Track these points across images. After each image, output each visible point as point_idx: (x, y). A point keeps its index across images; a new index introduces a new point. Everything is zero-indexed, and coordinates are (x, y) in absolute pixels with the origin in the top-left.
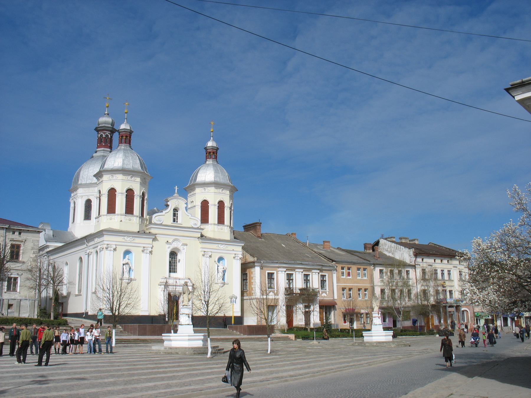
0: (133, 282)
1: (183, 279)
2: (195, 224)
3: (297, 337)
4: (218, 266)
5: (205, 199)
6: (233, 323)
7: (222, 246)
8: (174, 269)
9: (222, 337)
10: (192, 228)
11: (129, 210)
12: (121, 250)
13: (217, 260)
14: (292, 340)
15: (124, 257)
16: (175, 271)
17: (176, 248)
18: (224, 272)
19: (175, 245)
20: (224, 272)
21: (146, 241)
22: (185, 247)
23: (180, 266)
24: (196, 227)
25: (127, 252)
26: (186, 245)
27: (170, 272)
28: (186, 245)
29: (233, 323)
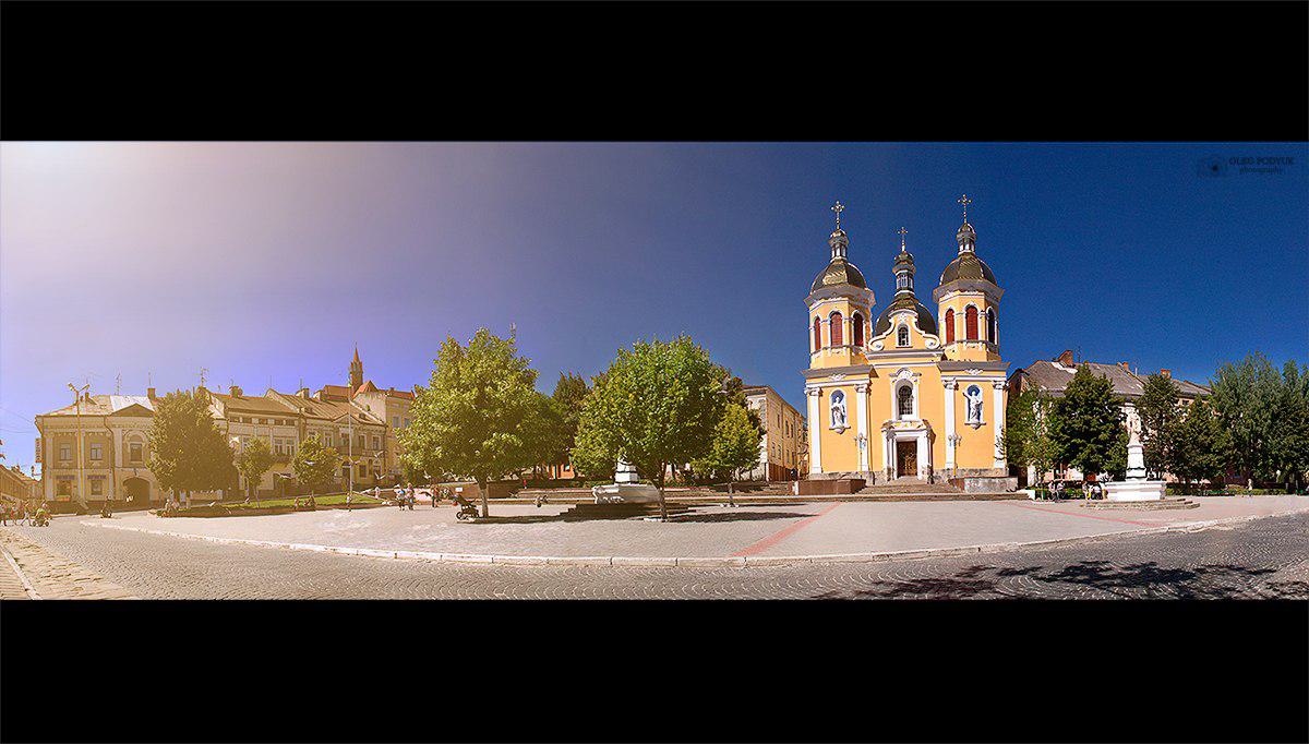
4: (969, 401)
12: (828, 393)
13: (966, 393)
18: (978, 406)
19: (903, 375)
20: (978, 406)
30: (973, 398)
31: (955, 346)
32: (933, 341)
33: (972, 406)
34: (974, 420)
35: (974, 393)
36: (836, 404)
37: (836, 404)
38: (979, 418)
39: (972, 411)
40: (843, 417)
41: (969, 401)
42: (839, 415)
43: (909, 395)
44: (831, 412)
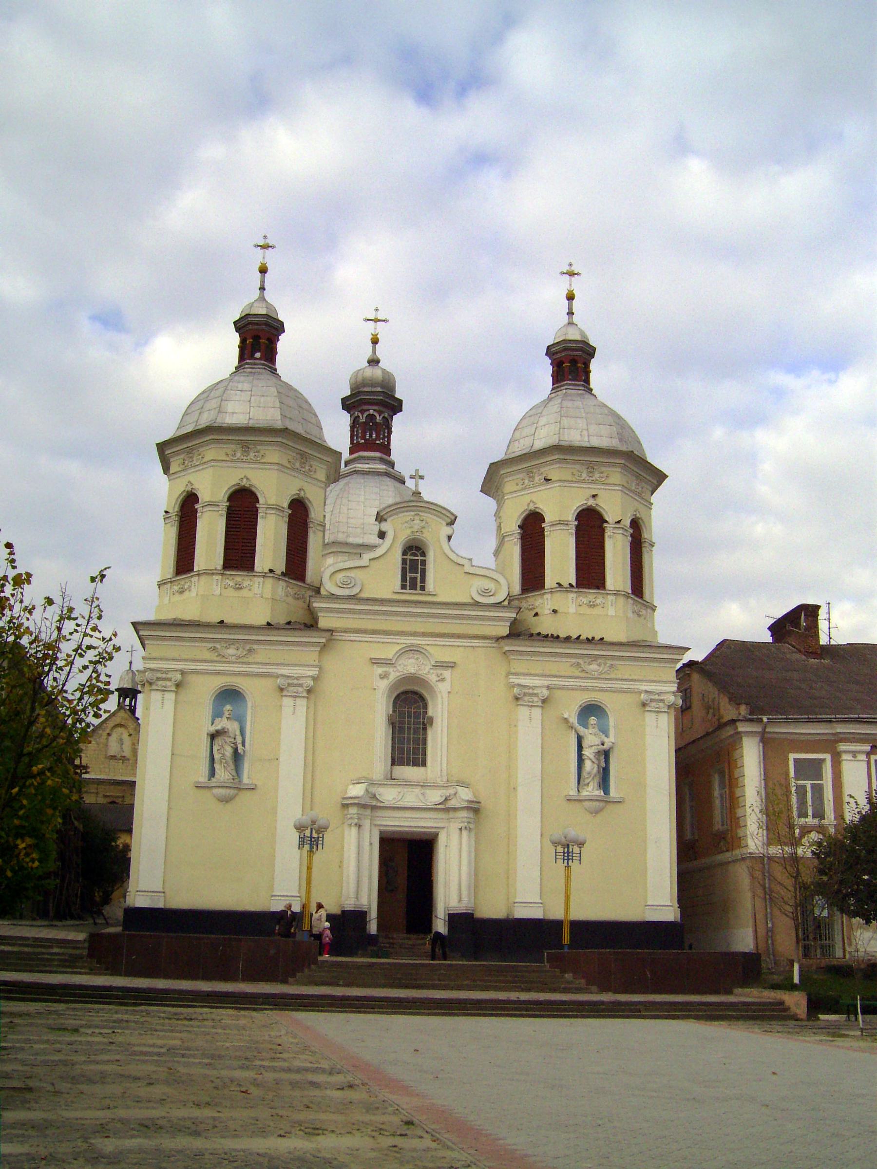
0: (245, 796)
1: (436, 787)
2: (486, 592)
3: (816, 1006)
5: (532, 507)
6: (566, 938)
7: (594, 667)
8: (416, 750)
9: (524, 996)
10: (477, 604)
11: (239, 554)
12: (205, 688)
13: (574, 720)
14: (795, 1018)
15: (217, 714)
17: (413, 679)
18: (606, 754)
19: (410, 666)
21: (296, 659)
22: (447, 673)
23: (438, 740)
24: (492, 600)
25: (230, 696)
26: (451, 666)
27: (393, 763)
28: (451, 666)
29: (566, 938)
30: (592, 740)
31: (544, 602)
33: (588, 752)
34: (592, 790)
36: (222, 723)
39: (588, 765)
42: (229, 751)
43: (417, 715)
44: (205, 741)
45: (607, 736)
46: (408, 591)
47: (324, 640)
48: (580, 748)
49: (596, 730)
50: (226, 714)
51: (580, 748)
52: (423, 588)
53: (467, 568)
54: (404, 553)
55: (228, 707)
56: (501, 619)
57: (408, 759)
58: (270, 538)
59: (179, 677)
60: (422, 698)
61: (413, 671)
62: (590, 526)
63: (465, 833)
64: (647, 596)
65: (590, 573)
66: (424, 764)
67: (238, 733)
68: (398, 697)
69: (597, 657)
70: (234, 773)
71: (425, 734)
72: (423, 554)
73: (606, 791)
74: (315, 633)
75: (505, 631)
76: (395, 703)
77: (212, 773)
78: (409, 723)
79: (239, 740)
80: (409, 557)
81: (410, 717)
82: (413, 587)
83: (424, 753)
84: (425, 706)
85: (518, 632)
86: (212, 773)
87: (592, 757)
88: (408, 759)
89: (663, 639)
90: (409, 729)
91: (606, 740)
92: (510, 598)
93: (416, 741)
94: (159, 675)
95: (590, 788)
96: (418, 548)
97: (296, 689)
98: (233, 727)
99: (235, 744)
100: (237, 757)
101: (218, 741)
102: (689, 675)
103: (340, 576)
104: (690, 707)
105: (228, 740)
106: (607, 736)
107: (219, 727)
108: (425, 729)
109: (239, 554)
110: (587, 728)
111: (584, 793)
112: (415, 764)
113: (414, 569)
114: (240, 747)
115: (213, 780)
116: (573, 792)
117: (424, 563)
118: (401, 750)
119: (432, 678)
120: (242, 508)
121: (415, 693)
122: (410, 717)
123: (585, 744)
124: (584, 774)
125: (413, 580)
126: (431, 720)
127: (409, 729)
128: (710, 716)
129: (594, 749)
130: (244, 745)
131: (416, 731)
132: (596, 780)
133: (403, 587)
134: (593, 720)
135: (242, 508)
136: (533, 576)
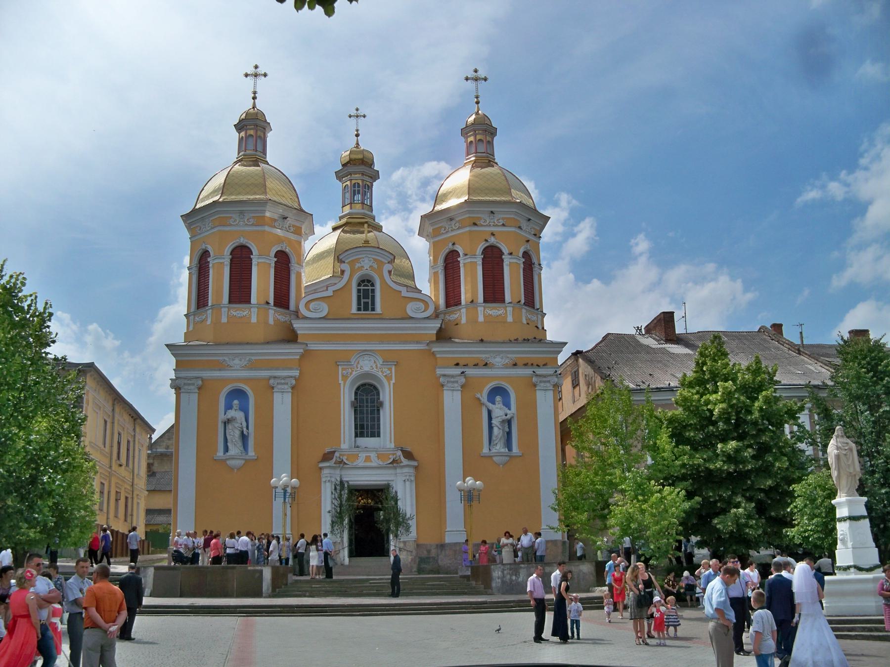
4: (490, 413)
7: (498, 359)
8: (373, 427)
11: (240, 291)
13: (484, 399)
15: (229, 407)
16: (376, 434)
18: (509, 422)
27: (356, 436)
30: (499, 411)
31: (462, 315)
32: (422, 305)
33: (495, 422)
34: (500, 448)
35: (498, 398)
36: (231, 413)
37: (231, 413)
38: (508, 444)
39: (496, 431)
40: (244, 438)
41: (490, 413)
42: (237, 433)
43: (373, 401)
45: (510, 409)
46: (362, 312)
47: (302, 351)
48: (490, 418)
49: (501, 405)
50: (235, 407)
51: (490, 418)
52: (373, 309)
53: (405, 293)
54: (359, 285)
55: (236, 402)
56: (431, 329)
57: (367, 432)
58: (262, 282)
59: (200, 382)
60: (375, 388)
61: (367, 369)
62: (492, 259)
63: (407, 483)
64: (537, 306)
65: (493, 292)
66: (379, 436)
67: (244, 420)
68: (358, 389)
69: (500, 352)
70: (242, 448)
71: (379, 414)
72: (373, 285)
73: (510, 449)
74: (296, 346)
75: (434, 338)
76: (356, 393)
77: (226, 449)
78: (367, 406)
79: (244, 424)
80: (362, 288)
81: (367, 402)
82: (366, 309)
83: (379, 428)
84: (378, 394)
85: (442, 336)
86: (226, 449)
87: (498, 424)
88: (367, 432)
89: (549, 337)
90: (367, 410)
91: (508, 412)
92: (436, 315)
93: (373, 419)
94: (186, 381)
95: (498, 447)
96: (369, 281)
97: (283, 387)
98: (240, 415)
99: (242, 428)
100: (244, 438)
101: (229, 427)
102: (577, 361)
103: (311, 306)
104: (578, 385)
105: (237, 425)
106: (510, 409)
107: (229, 417)
108: (378, 410)
109: (240, 291)
110: (494, 403)
111: (494, 451)
112: (373, 435)
113: (366, 296)
114: (245, 429)
115: (228, 454)
116: (485, 450)
117: (373, 291)
118: (362, 427)
119: (380, 375)
120: (241, 259)
121: (371, 385)
122: (367, 402)
123: (494, 415)
124: (494, 438)
125: (366, 304)
126: (381, 404)
127: (367, 410)
128: (590, 390)
129: (500, 419)
130: (247, 428)
131: (372, 412)
132: (503, 441)
133: (359, 309)
134: (498, 398)
135: (241, 259)
136: (452, 297)
